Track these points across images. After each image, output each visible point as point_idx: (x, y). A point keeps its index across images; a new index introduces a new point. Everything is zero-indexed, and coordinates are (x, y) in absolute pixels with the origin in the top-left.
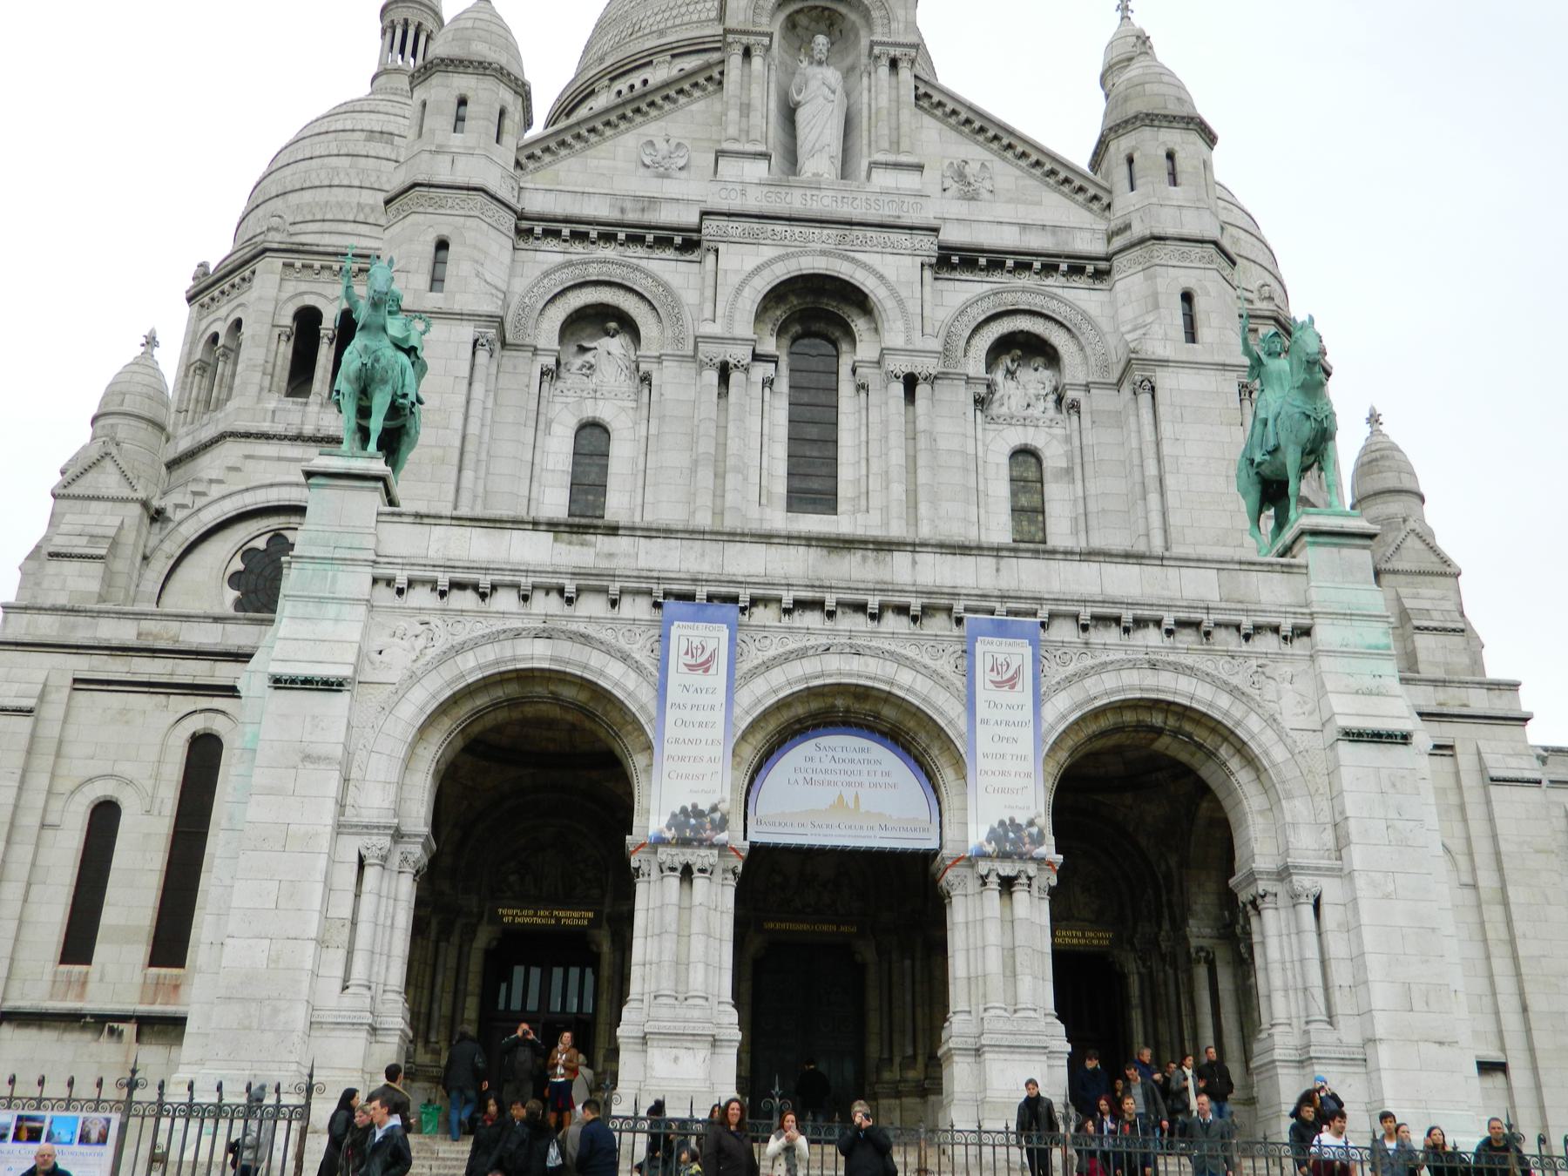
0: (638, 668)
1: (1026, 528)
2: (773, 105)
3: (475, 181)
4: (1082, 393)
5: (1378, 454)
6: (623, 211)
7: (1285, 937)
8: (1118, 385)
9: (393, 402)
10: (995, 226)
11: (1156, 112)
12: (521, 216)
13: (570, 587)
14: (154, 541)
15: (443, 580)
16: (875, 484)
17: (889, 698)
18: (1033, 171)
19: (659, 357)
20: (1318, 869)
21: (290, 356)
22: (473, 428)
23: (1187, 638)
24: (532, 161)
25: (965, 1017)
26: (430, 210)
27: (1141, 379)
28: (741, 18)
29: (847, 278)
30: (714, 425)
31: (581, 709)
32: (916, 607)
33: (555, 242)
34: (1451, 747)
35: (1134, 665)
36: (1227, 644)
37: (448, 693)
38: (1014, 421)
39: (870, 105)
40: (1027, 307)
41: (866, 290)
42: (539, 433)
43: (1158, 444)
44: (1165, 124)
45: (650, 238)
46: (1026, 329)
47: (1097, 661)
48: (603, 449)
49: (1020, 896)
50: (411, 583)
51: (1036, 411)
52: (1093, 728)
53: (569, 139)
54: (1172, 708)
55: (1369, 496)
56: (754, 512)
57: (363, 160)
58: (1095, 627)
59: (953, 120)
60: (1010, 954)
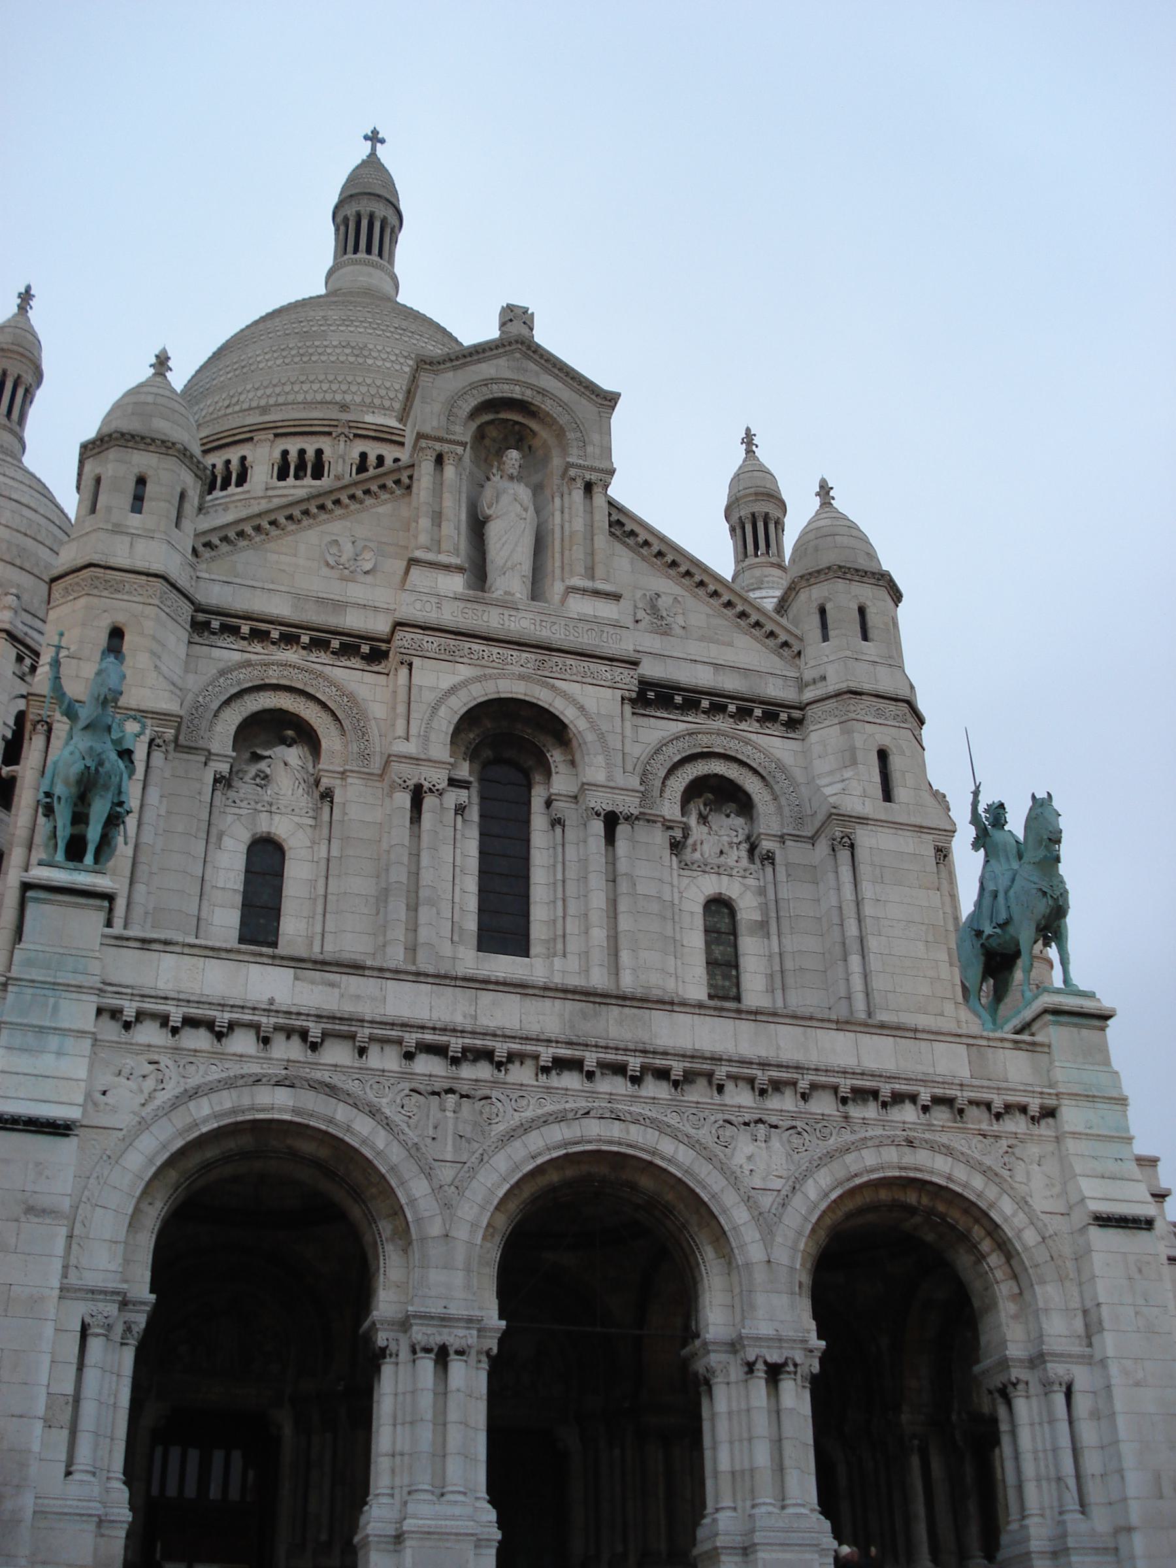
2: (464, 516)
3: (156, 567)
4: (777, 845)
7: (1037, 1427)
8: (813, 840)
10: (689, 665)
11: (848, 565)
12: (199, 608)
13: (315, 1030)
15: (176, 1015)
16: (572, 927)
18: (725, 611)
19: (343, 773)
23: (941, 1115)
25: (730, 1513)
26: (105, 593)
27: (841, 835)
28: (435, 424)
29: (546, 706)
30: (406, 853)
33: (232, 639)
36: (980, 1122)
37: (179, 1143)
39: (562, 528)
40: (722, 751)
41: (566, 721)
42: (211, 847)
43: (858, 904)
44: (857, 578)
46: (721, 773)
50: (140, 1016)
51: (731, 859)
52: (850, 1205)
54: (928, 1187)
56: (446, 949)
58: (854, 1100)
59: (644, 551)
60: (778, 1442)
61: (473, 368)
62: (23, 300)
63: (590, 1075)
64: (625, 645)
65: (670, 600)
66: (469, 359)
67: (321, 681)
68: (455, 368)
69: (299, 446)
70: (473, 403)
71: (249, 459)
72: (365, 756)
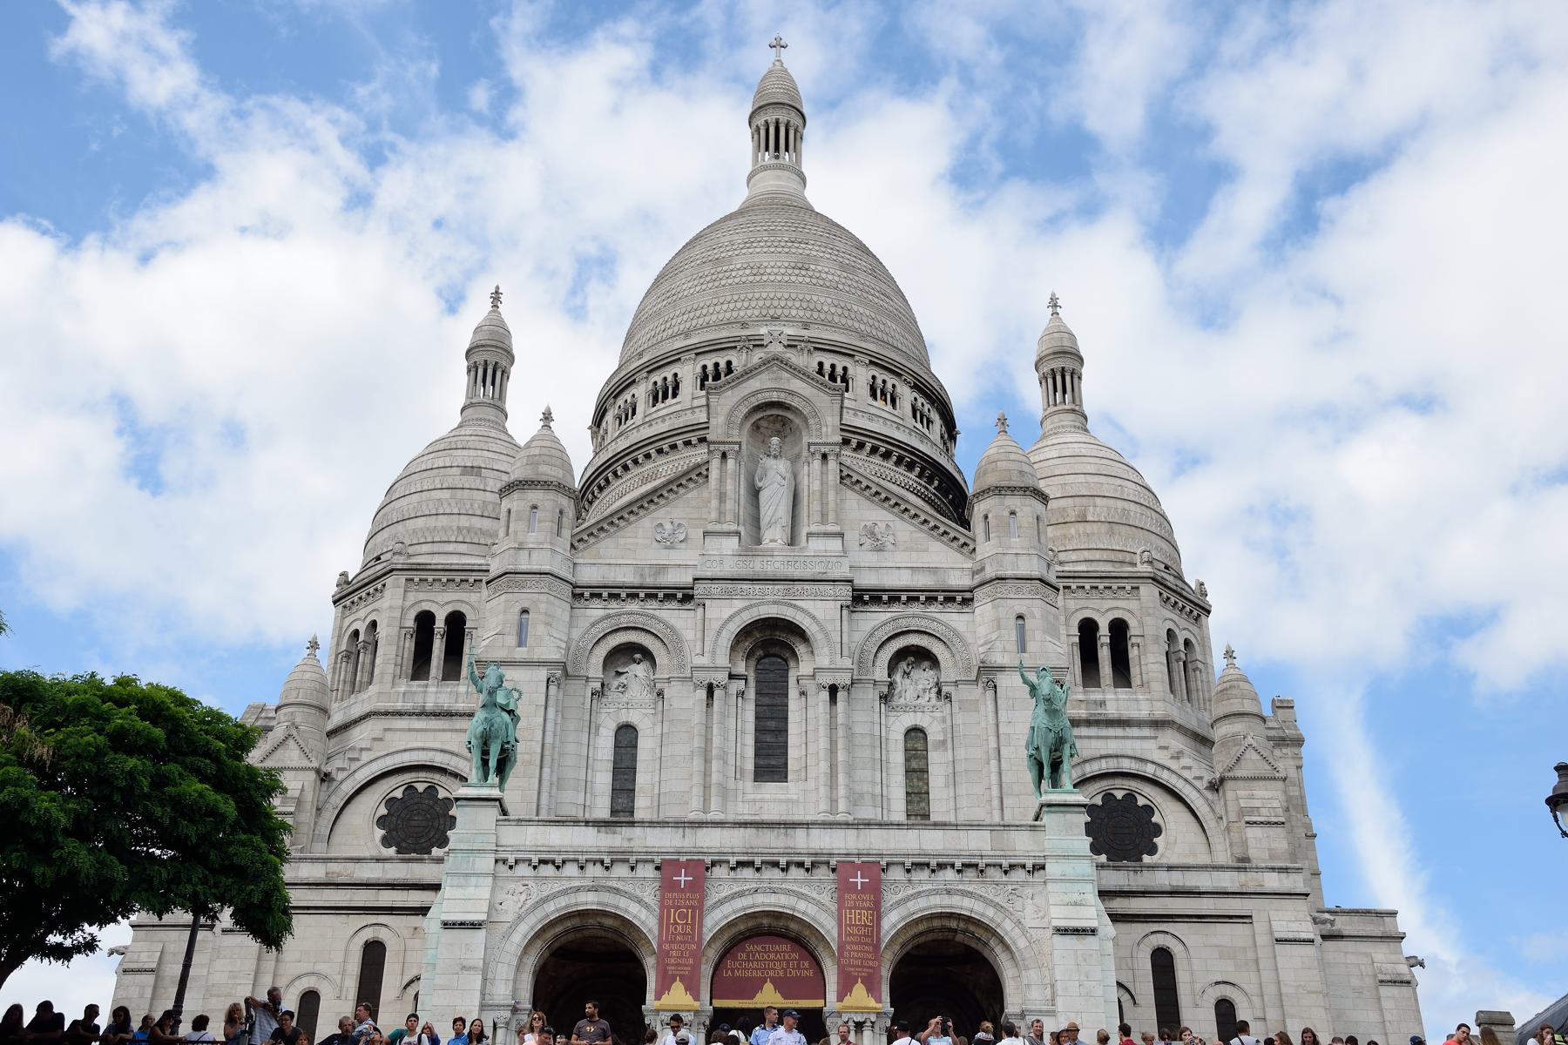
0: (647, 906)
1: (916, 784)
3: (546, 568)
4: (953, 688)
5: (1227, 685)
6: (642, 575)
9: (502, 746)
13: (607, 860)
14: (323, 796)
17: (793, 918)
18: (923, 527)
20: (1041, 1011)
21: (413, 649)
22: (549, 740)
23: (970, 874)
24: (581, 543)
28: (719, 431)
31: (616, 931)
32: (808, 864)
33: (598, 601)
34: (1250, 917)
35: (937, 892)
36: (994, 877)
38: (908, 709)
40: (916, 628)
45: (661, 595)
47: (914, 891)
48: (634, 743)
49: (867, 1033)
52: (915, 930)
53: (606, 527)
55: (1221, 718)
57: (460, 492)
59: (867, 493)
61: (744, 385)
62: (494, 299)
63: (758, 870)
64: (842, 571)
65: (884, 526)
66: (741, 379)
67: (654, 620)
68: (732, 388)
69: (714, 361)
70: (745, 411)
71: (679, 376)
72: (681, 666)
